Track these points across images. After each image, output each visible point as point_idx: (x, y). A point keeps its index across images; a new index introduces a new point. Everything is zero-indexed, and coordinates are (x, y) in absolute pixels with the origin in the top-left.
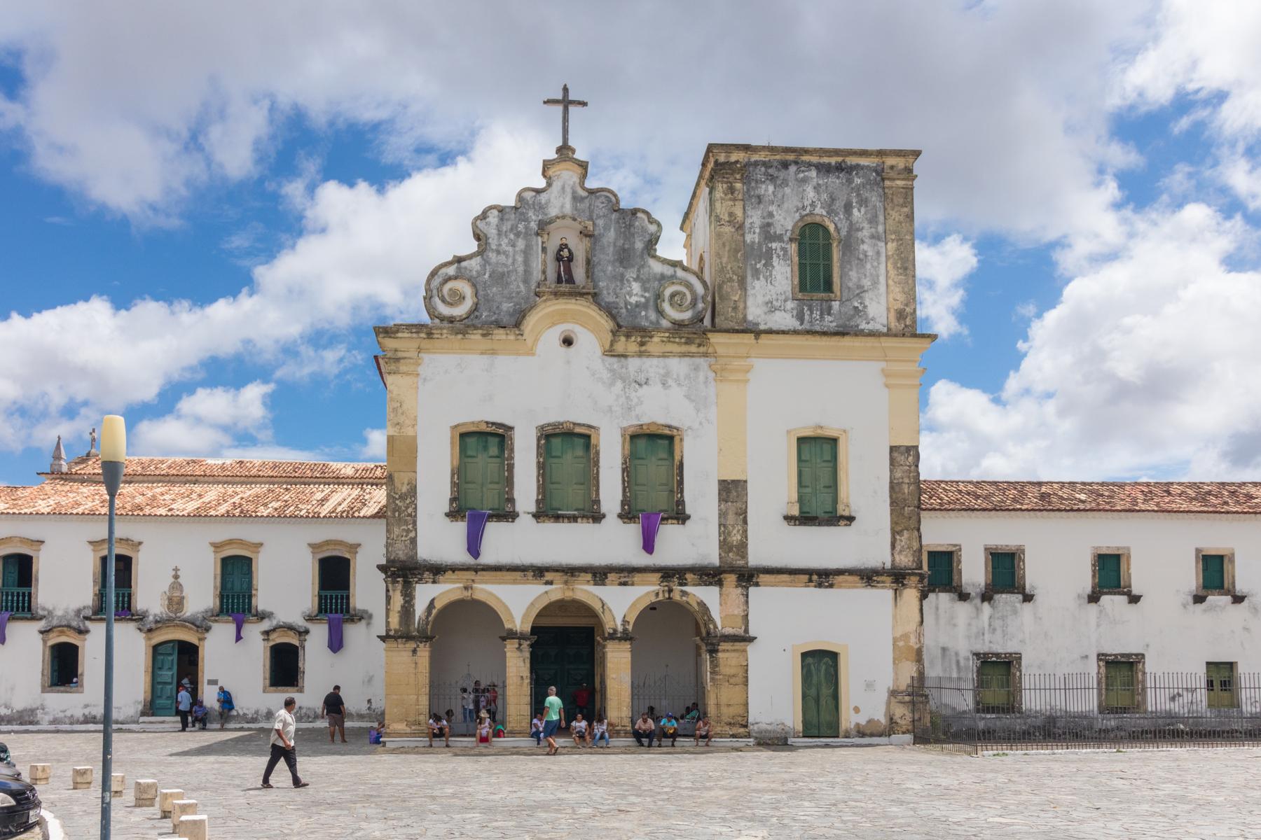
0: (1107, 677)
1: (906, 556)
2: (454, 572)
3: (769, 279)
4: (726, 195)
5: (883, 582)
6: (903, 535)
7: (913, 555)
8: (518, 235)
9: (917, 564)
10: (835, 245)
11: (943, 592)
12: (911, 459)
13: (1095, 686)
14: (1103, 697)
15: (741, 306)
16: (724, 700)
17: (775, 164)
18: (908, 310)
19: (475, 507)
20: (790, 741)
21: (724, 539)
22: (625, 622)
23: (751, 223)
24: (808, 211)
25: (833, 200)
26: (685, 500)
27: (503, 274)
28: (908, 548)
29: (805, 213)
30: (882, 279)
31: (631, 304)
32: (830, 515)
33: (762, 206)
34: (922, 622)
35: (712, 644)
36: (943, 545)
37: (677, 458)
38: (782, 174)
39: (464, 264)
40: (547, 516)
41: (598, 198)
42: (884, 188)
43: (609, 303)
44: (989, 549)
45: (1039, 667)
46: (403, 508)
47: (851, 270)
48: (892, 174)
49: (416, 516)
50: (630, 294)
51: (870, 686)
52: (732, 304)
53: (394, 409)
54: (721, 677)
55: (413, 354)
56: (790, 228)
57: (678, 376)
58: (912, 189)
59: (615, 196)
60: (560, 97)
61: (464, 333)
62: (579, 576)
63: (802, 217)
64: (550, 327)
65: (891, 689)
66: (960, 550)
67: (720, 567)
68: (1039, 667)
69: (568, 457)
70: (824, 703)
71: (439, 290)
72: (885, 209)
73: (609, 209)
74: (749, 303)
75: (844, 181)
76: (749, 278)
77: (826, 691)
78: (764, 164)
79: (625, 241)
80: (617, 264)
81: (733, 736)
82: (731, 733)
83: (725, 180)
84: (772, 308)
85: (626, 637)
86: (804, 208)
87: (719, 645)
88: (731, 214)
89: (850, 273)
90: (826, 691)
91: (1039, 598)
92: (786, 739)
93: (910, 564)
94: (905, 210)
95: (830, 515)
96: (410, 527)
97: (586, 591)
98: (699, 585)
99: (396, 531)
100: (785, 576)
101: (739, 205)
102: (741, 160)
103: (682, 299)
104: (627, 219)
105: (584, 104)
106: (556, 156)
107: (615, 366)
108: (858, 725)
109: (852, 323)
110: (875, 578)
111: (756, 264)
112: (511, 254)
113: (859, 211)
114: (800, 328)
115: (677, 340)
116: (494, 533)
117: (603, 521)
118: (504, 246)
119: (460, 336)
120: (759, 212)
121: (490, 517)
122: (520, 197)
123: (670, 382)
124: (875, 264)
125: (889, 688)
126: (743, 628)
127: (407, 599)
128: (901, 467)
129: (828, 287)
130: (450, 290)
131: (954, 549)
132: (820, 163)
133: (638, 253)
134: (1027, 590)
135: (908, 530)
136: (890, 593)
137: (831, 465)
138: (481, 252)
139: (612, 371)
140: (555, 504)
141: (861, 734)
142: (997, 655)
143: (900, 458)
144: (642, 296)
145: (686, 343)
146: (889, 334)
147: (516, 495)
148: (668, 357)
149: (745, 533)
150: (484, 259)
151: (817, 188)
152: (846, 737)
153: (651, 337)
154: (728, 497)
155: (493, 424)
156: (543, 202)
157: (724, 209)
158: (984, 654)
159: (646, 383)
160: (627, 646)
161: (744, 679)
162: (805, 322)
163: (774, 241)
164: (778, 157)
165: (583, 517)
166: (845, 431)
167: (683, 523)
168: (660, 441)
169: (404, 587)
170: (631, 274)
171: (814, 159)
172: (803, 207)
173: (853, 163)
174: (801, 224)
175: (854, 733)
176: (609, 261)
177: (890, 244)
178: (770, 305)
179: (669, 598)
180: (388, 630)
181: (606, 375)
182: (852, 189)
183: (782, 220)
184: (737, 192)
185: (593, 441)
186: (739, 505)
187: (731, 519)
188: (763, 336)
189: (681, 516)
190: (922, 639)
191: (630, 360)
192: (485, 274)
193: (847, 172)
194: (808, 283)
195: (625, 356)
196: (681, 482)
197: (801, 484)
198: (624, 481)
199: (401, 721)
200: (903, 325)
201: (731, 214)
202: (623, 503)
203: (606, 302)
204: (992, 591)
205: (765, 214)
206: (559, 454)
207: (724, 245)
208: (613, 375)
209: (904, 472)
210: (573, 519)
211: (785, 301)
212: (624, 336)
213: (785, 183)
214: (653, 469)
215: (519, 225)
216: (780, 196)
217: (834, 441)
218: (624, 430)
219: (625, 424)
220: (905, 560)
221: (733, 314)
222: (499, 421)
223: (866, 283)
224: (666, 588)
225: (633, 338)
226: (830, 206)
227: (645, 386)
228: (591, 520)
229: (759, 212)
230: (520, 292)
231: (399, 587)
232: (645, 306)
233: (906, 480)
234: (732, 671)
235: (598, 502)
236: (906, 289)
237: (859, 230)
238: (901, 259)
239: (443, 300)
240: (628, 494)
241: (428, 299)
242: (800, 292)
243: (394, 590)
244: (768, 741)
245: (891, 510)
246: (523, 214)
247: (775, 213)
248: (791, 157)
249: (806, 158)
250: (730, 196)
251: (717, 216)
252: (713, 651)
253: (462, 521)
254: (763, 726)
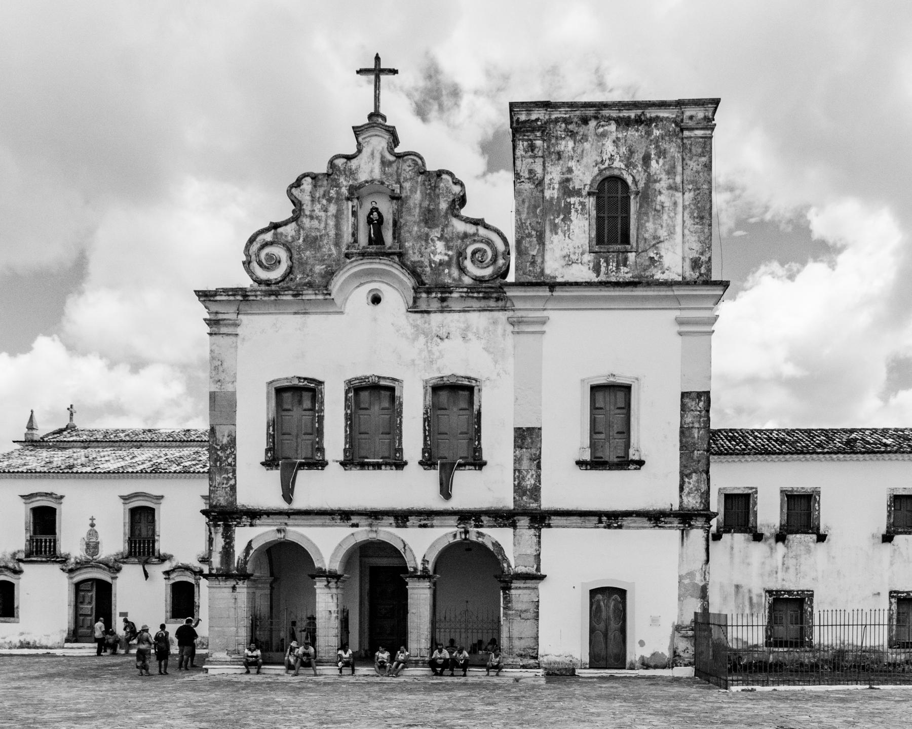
0: (898, 613)
1: (694, 498)
2: (268, 516)
3: (567, 233)
4: (526, 152)
5: (671, 523)
6: (692, 478)
7: (701, 497)
8: (330, 200)
9: (705, 505)
10: (632, 197)
11: (738, 532)
12: (701, 404)
13: (886, 622)
14: (894, 632)
15: (539, 260)
16: (515, 634)
17: (576, 120)
18: (703, 258)
19: (290, 456)
20: (578, 671)
21: (519, 483)
22: (425, 561)
23: (551, 180)
24: (606, 165)
25: (631, 152)
26: (483, 446)
27: (316, 238)
28: (697, 490)
29: (603, 167)
30: (679, 229)
31: (435, 262)
32: (623, 459)
33: (561, 162)
34: (707, 561)
35: (505, 582)
36: (739, 488)
37: (476, 407)
38: (582, 130)
39: (280, 230)
40: (353, 463)
41: (405, 161)
42: (682, 139)
43: (415, 262)
44: (785, 491)
45: (831, 604)
46: (224, 459)
47: (648, 221)
48: (691, 124)
49: (235, 465)
50: (434, 253)
51: (655, 621)
52: (530, 259)
53: (215, 367)
54: (514, 612)
55: (233, 316)
56: (589, 182)
57: (477, 329)
58: (711, 138)
59: (421, 158)
60: (371, 65)
61: (276, 294)
62: (382, 519)
63: (601, 171)
64: (358, 286)
65: (676, 624)
66: (756, 492)
67: (514, 509)
68: (831, 604)
69: (376, 408)
70: (612, 636)
71: (258, 255)
72: (683, 159)
73: (415, 172)
74: (548, 256)
75: (643, 133)
76: (548, 234)
77: (614, 625)
78: (567, 121)
79: (430, 202)
80: (422, 224)
81: (524, 667)
82: (521, 664)
83: (526, 137)
84: (569, 261)
85: (425, 575)
86: (602, 162)
87: (511, 583)
88: (531, 171)
89: (647, 224)
90: (614, 625)
91: (832, 537)
92: (574, 670)
93: (698, 505)
94: (703, 159)
95: (623, 459)
96: (230, 475)
97: (388, 532)
98: (494, 526)
99: (218, 479)
100: (575, 518)
101: (539, 161)
102: (541, 118)
103: (483, 256)
104: (433, 181)
105: (394, 72)
106: (367, 121)
107: (419, 322)
108: (642, 657)
109: (648, 274)
110: (663, 519)
111: (554, 219)
112: (324, 219)
113: (657, 162)
114: (596, 280)
115: (475, 295)
116: (305, 478)
117: (405, 468)
118: (317, 211)
119: (273, 298)
120: (559, 168)
121: (301, 466)
122: (331, 163)
123: (470, 335)
124: (672, 214)
125: (674, 623)
126: (535, 566)
127: (228, 540)
128: (692, 413)
129: (626, 239)
130: (267, 254)
131: (750, 492)
132: (619, 117)
133: (442, 214)
134: (822, 531)
135: (695, 472)
136: (678, 533)
137: (624, 411)
138: (296, 217)
139: (416, 326)
140: (363, 453)
141: (646, 665)
142: (790, 592)
143: (691, 404)
144: (446, 254)
145: (484, 298)
146: (685, 283)
147: (325, 446)
148: (468, 311)
149: (539, 476)
150: (298, 225)
151: (616, 142)
152: (632, 668)
153: (451, 292)
154: (523, 443)
155: (305, 379)
156: (353, 168)
157: (524, 166)
158: (777, 591)
159: (447, 337)
160: (427, 584)
161: (535, 614)
162: (602, 273)
163: (573, 196)
164: (578, 113)
165: (386, 464)
166: (637, 379)
167: (480, 469)
168: (461, 392)
169: (224, 530)
170: (435, 233)
171: (614, 114)
172: (602, 160)
173: (653, 115)
174: (600, 178)
175: (638, 664)
176: (414, 222)
177: (687, 194)
178: (567, 259)
179: (466, 539)
180: (211, 569)
181: (409, 330)
182: (651, 141)
183: (581, 175)
184: (537, 150)
185: (397, 393)
186: (533, 451)
187: (525, 464)
188: (557, 288)
189: (478, 464)
190: (707, 577)
191: (432, 315)
192: (299, 239)
193: (646, 125)
194: (606, 235)
195: (428, 312)
196: (478, 431)
197: (594, 430)
198: (425, 430)
199: (222, 650)
200: (698, 274)
201: (531, 171)
202: (424, 452)
203: (411, 261)
204: (786, 531)
205: (565, 170)
206: (367, 406)
207: (523, 202)
208: (417, 330)
209: (694, 417)
210: (378, 466)
211: (582, 254)
212: (425, 292)
213: (585, 138)
214: (455, 419)
215: (331, 191)
216: (579, 151)
217: (627, 389)
218: (426, 382)
219: (427, 377)
220: (693, 502)
221: (531, 269)
222: (310, 376)
223: (662, 233)
224: (463, 530)
225: (434, 295)
226: (629, 159)
227: (446, 340)
228: (394, 467)
229: (559, 168)
230: (332, 254)
231: (221, 529)
232: (448, 264)
233: (697, 425)
234: (523, 607)
235: (400, 450)
236: (702, 238)
237: (656, 181)
238: (698, 208)
239: (260, 264)
240: (429, 443)
241: (247, 264)
242: (597, 245)
243: (216, 533)
244: (556, 672)
245: (681, 454)
246: (335, 180)
247: (574, 168)
248: (591, 112)
249: (606, 112)
250: (530, 153)
251: (518, 174)
252: (507, 588)
253: (277, 469)
254: (552, 658)
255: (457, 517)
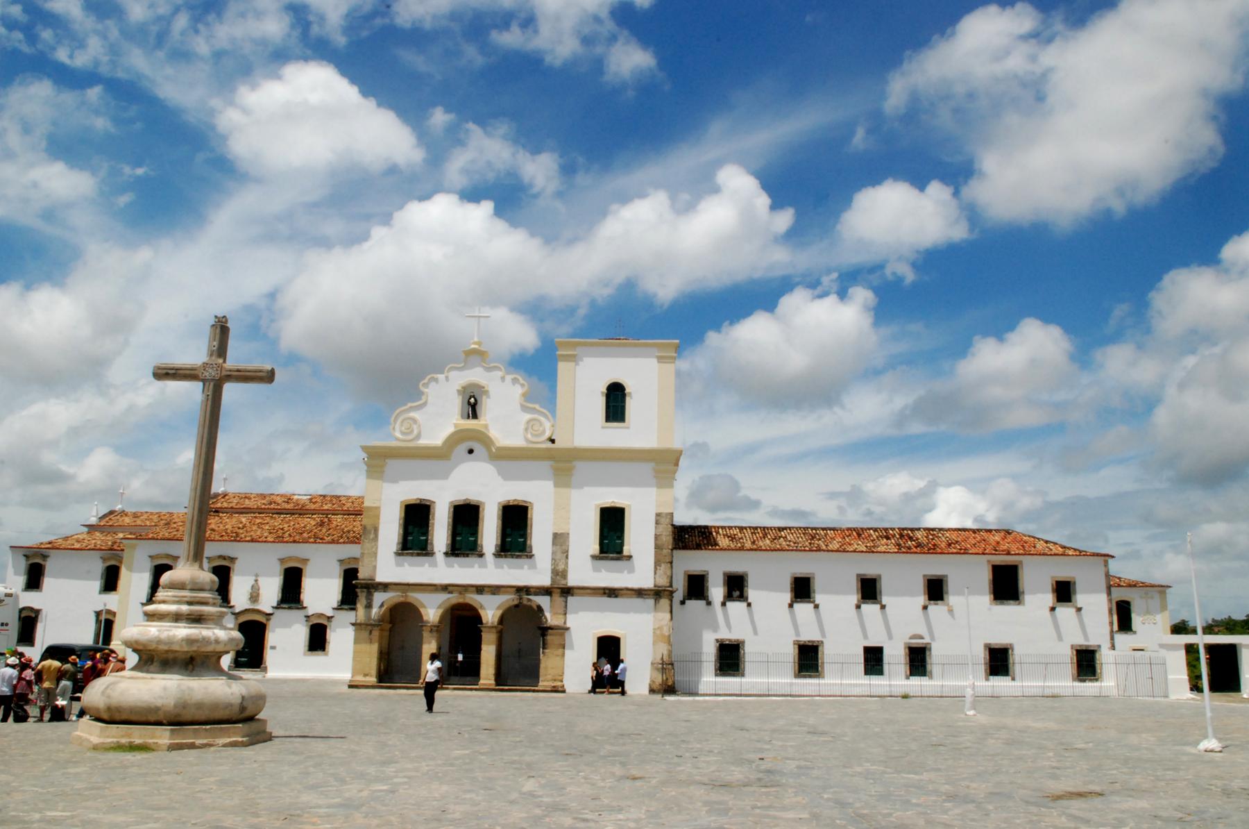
5: (649, 595)
97: (474, 599)
126: (563, 621)
149: (567, 563)
187: (559, 555)
218: (499, 503)
220: (663, 581)
245: (655, 552)
255: (514, 589)
